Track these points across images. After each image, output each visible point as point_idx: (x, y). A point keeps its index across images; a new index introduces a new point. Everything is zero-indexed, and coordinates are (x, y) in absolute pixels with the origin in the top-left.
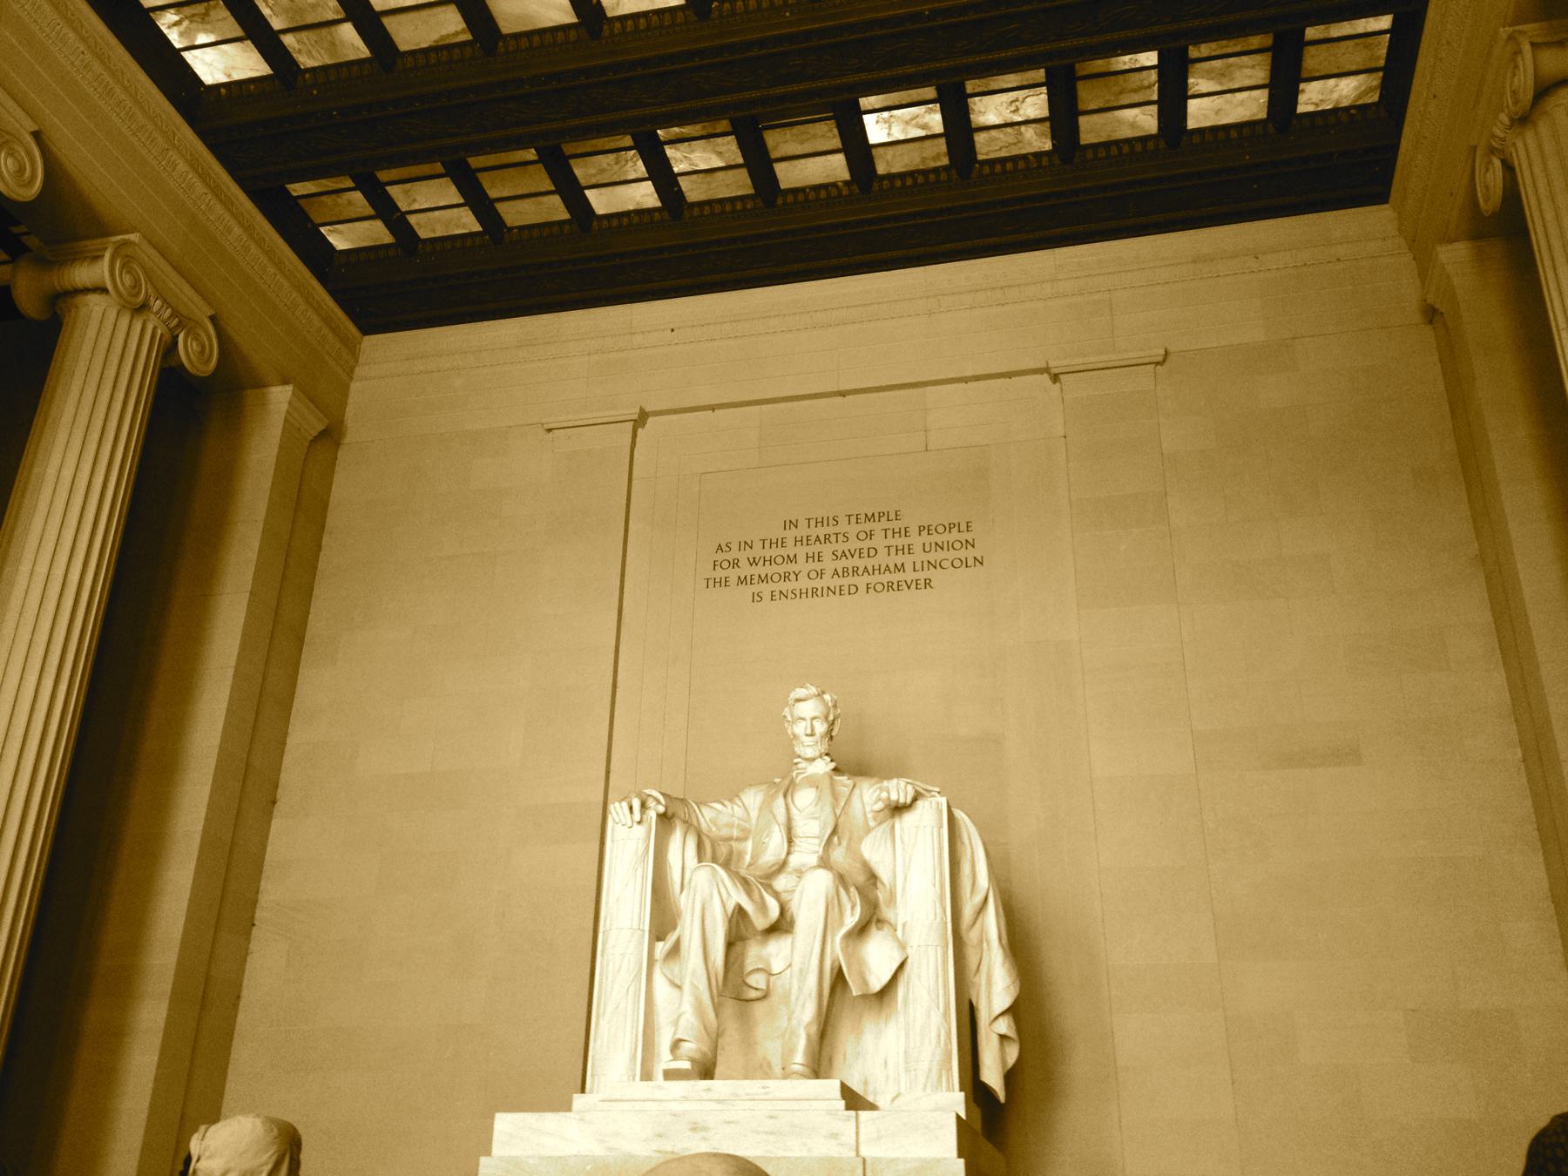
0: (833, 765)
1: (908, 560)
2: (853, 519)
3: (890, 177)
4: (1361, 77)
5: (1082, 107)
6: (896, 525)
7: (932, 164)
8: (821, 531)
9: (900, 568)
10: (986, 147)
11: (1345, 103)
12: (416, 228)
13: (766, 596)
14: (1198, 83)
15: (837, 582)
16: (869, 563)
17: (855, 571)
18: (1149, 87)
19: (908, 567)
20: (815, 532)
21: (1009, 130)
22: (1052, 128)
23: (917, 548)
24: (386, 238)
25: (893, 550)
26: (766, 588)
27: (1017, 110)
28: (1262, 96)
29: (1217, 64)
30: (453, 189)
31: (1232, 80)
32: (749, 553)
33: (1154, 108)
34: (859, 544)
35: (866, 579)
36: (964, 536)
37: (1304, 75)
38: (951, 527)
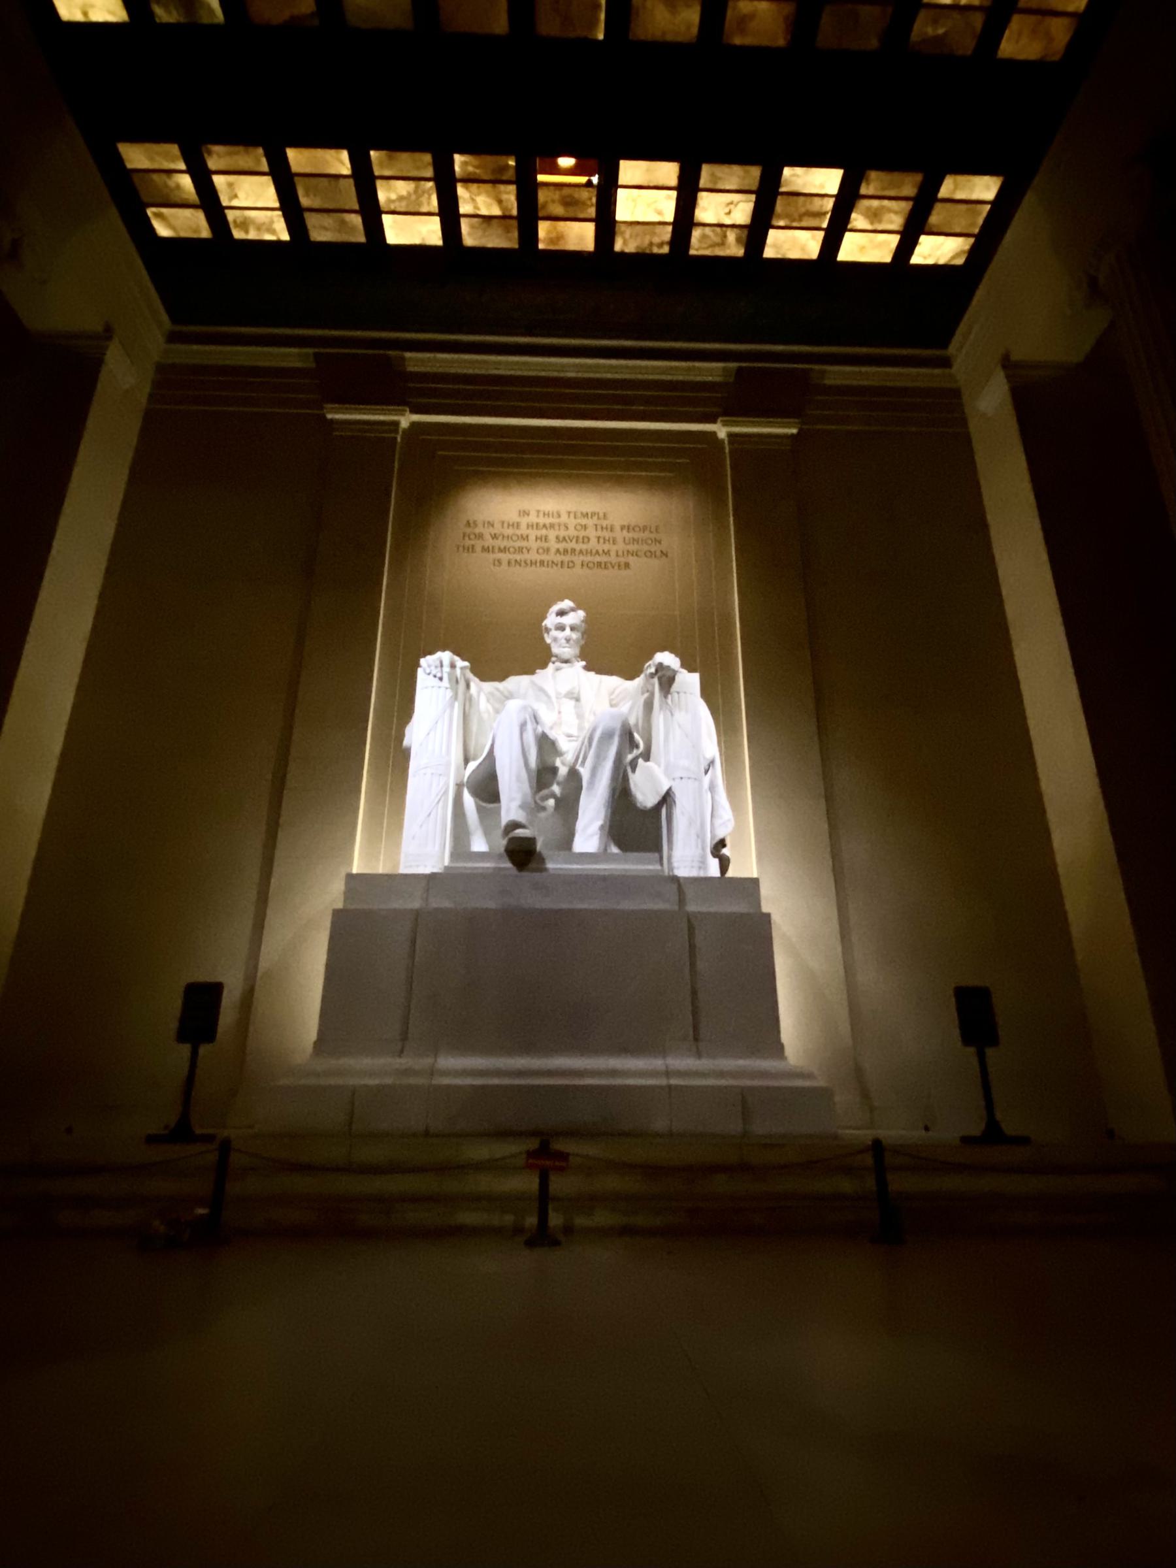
0: (584, 663)
1: (614, 548)
2: (572, 515)
3: (622, 254)
4: (960, 240)
5: (775, 222)
6: (604, 523)
7: (656, 250)
8: (548, 521)
9: (607, 553)
10: (699, 244)
11: (942, 262)
12: (232, 226)
13: (505, 563)
14: (858, 220)
15: (559, 558)
16: (584, 547)
17: (573, 550)
18: (825, 213)
19: (613, 554)
20: (542, 520)
21: (718, 229)
22: (749, 236)
23: (620, 540)
24: (205, 233)
25: (601, 541)
26: (504, 557)
27: (729, 213)
28: (895, 240)
29: (875, 203)
30: (272, 190)
31: (880, 222)
32: (493, 531)
33: (821, 234)
34: (576, 533)
35: (582, 558)
36: (653, 536)
37: (927, 229)
38: (644, 529)
